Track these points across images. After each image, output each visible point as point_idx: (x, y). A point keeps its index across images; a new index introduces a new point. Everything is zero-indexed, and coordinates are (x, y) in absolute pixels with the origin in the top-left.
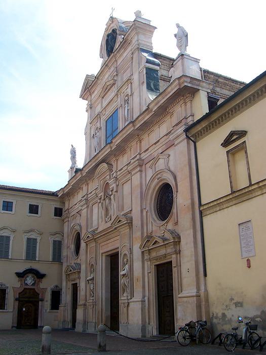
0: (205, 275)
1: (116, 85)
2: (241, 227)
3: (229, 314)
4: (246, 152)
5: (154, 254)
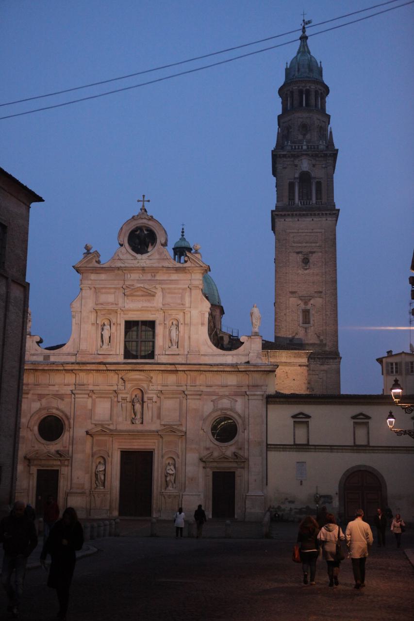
0: (267, 485)
3: (283, 507)
4: (308, 427)
5: (215, 464)
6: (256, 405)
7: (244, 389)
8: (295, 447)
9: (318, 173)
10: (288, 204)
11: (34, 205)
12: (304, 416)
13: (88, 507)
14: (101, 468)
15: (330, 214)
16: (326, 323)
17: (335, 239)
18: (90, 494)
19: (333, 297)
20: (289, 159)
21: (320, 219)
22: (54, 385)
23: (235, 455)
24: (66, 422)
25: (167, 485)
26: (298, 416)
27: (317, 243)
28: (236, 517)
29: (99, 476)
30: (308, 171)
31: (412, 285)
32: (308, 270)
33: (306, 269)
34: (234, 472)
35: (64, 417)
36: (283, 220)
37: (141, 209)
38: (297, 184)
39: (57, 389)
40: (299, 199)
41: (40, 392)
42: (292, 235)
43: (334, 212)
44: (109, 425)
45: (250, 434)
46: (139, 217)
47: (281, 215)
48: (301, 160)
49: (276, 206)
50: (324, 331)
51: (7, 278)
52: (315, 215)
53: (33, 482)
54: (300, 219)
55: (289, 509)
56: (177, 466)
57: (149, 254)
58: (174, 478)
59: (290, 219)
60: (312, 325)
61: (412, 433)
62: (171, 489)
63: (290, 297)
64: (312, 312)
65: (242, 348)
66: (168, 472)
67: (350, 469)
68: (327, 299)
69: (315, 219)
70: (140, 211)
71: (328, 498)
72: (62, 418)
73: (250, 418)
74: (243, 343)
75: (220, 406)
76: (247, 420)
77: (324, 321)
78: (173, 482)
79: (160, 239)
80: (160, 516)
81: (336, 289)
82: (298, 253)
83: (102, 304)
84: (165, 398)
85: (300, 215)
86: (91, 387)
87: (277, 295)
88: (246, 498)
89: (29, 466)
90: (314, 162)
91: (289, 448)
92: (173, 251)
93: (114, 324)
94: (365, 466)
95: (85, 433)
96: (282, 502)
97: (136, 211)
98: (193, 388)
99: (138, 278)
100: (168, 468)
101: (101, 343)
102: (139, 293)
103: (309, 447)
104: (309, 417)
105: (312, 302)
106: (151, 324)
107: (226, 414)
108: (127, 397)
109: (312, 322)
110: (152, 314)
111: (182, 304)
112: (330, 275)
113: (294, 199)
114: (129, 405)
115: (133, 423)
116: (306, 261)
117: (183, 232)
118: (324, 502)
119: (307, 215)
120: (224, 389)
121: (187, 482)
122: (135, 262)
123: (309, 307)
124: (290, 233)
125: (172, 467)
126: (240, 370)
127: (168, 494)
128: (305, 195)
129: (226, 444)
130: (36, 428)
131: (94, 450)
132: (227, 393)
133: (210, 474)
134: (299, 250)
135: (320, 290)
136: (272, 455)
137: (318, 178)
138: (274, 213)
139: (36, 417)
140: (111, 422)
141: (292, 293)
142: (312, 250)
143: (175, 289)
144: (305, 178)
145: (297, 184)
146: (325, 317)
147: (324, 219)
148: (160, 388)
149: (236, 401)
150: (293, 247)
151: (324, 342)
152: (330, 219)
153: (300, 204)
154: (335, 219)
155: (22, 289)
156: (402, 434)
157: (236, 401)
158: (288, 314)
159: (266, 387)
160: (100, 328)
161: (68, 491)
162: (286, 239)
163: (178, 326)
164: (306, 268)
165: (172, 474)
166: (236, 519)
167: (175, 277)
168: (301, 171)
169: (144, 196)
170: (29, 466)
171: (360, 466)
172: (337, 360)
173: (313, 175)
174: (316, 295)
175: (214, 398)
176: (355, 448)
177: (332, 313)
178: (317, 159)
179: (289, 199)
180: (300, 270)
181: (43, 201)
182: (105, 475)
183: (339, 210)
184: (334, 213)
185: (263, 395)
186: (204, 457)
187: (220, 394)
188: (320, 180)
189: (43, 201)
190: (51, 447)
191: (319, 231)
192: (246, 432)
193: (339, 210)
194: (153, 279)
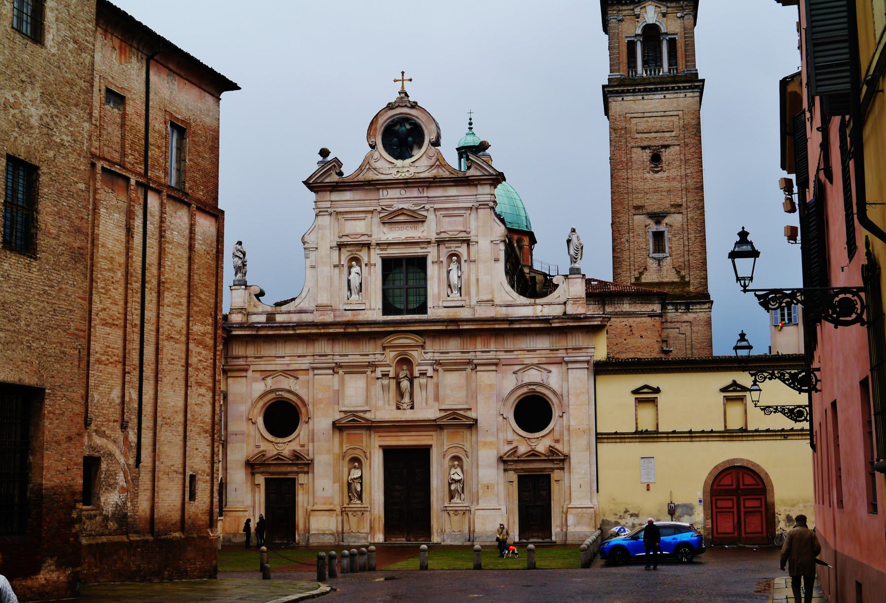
0: (598, 492)
1: (426, 224)
2: (643, 460)
6: (580, 377)
7: (562, 353)
8: (637, 436)
9: (670, 26)
10: (626, 75)
11: (225, 96)
12: (650, 391)
13: (340, 529)
14: (356, 473)
15: (690, 87)
16: (689, 251)
17: (699, 124)
18: (342, 512)
19: (698, 212)
20: (624, 8)
21: (675, 95)
22: (283, 357)
23: (552, 451)
24: (303, 410)
25: (452, 497)
26: (641, 391)
27: (673, 131)
28: (554, 538)
29: (353, 486)
30: (655, 24)
31: (785, 191)
32: (660, 173)
33: (657, 172)
34: (550, 475)
35: (299, 403)
36: (620, 99)
37: (400, 93)
38: (639, 44)
39: (289, 362)
40: (643, 66)
41: (263, 368)
42: (634, 121)
43: (696, 84)
44: (365, 412)
45: (571, 420)
46: (397, 104)
47: (617, 91)
48: (645, 7)
49: (609, 79)
50: (686, 263)
51: (189, 205)
52: (667, 89)
53: (261, 496)
54: (645, 97)
55: (631, 525)
56: (465, 468)
57: (413, 159)
58: (461, 486)
59: (631, 98)
60: (668, 255)
61: (787, 411)
62: (459, 501)
63: (634, 215)
64: (667, 235)
65: (556, 294)
66: (453, 476)
67: (720, 464)
68: (689, 215)
69: (668, 96)
70: (399, 96)
71: (689, 509)
72: (296, 404)
73: (570, 396)
74: (557, 286)
75: (526, 380)
76: (565, 398)
77: (686, 249)
78: (460, 492)
79: (429, 136)
80: (444, 541)
81: (702, 200)
82: (644, 148)
83: (347, 236)
84: (445, 370)
85: (645, 90)
86: (338, 359)
87: (615, 213)
88: (567, 512)
89: (253, 474)
90: (664, 9)
91: (629, 438)
92: (456, 152)
93: (366, 265)
94: (742, 460)
96: (620, 516)
97: (393, 97)
98: (485, 355)
99: (398, 196)
100: (453, 471)
101: (349, 293)
102: (402, 218)
103: (659, 435)
104: (657, 391)
105: (666, 220)
106: (420, 263)
107: (534, 391)
108: (389, 371)
109: (667, 250)
110: (422, 248)
111: (465, 231)
112: (694, 178)
113: (635, 67)
114: (393, 383)
115: (398, 408)
116: (656, 159)
117: (470, 124)
119: (656, 90)
120: (531, 355)
121: (480, 491)
122: (394, 171)
123: (662, 228)
124: (631, 118)
125: (459, 470)
126: (553, 325)
127: (455, 509)
128: (652, 60)
129: (537, 435)
130: (260, 421)
131: (345, 449)
132: (536, 361)
133: (514, 477)
134: (645, 144)
135: (679, 201)
136: (603, 447)
137: (671, 34)
138: (606, 90)
139: (261, 403)
141: (637, 208)
142: (666, 143)
143: (454, 209)
144: (651, 33)
145: (639, 44)
146: (686, 243)
147: (682, 95)
148: (437, 356)
149: (550, 372)
150: (636, 138)
151: (687, 279)
152: (691, 94)
153: (645, 75)
154: (698, 94)
155: (213, 220)
156: (771, 412)
157: (550, 372)
158: (632, 240)
159: (592, 350)
160: (346, 269)
161: (310, 508)
162: (626, 128)
163: (459, 261)
164: (656, 169)
165: (459, 481)
166: (555, 542)
167: (453, 191)
168: (645, 24)
169: (403, 73)
170: (253, 474)
171: (733, 460)
172: (707, 306)
173: (663, 30)
174: (673, 210)
175: (517, 368)
176: (726, 434)
177: (697, 235)
178: (669, 5)
179: (629, 67)
180: (649, 172)
181: (239, 88)
182: (361, 484)
183: (703, 81)
184: (696, 85)
185: (588, 362)
186: (505, 454)
187: (527, 361)
188: (675, 36)
189: (239, 88)
190: (282, 446)
191: (675, 113)
192: (564, 415)
193: (703, 81)
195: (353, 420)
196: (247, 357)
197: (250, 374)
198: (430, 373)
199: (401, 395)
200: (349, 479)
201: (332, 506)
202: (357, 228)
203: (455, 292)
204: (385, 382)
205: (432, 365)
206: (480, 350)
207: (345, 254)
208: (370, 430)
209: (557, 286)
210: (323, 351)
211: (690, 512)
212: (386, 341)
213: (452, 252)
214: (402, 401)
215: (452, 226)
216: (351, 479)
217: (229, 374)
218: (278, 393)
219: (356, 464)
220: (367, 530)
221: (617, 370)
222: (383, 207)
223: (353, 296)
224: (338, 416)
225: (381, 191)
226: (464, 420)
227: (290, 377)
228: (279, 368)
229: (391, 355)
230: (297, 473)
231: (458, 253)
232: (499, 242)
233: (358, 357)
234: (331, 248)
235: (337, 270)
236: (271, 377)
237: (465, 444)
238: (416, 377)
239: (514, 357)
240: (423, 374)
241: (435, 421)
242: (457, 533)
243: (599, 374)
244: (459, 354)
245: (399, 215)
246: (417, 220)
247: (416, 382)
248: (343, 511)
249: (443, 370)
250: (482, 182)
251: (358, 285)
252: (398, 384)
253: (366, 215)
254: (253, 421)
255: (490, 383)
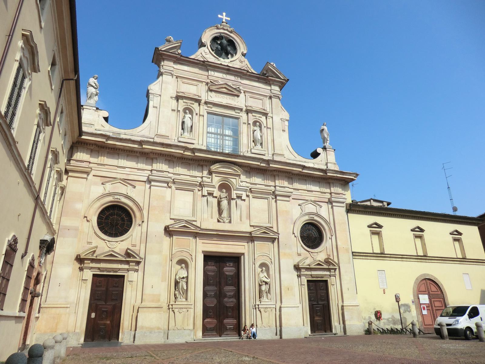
2: (379, 272)
24: (138, 214)
62: (267, 300)
74: (319, 154)
75: (307, 211)
93: (197, 114)
95: (163, 231)
114: (215, 201)
115: (219, 221)
118: (405, 312)
126: (328, 174)
127: (265, 306)
132: (313, 199)
139: (98, 204)
140: (194, 219)
149: (321, 207)
163: (260, 127)
170: (81, 269)
182: (187, 283)
194: (235, 80)
195: (185, 226)
196: (90, 163)
197: (90, 176)
198: (244, 197)
199: (220, 212)
200: (177, 277)
201: (160, 304)
202: (191, 90)
203: (259, 146)
204: (210, 198)
205: (246, 191)
206: (282, 185)
207: (182, 104)
208: (196, 237)
209: (319, 154)
210: (161, 168)
211: (409, 310)
212: (214, 167)
213: (256, 120)
214: (223, 216)
215: (256, 104)
216: (180, 278)
217: (70, 174)
218: (116, 197)
219: (183, 265)
220: (191, 327)
221: (360, 211)
222: (212, 81)
223: (186, 134)
224: (169, 222)
225: (210, 72)
226: (272, 234)
227: (128, 185)
228: (118, 176)
229: (216, 180)
230: (128, 270)
231: (262, 123)
232: (285, 120)
233: (188, 177)
234: (171, 98)
235: (175, 113)
236: (110, 183)
237: (270, 254)
238: (233, 199)
239: (299, 194)
240: (239, 197)
241: (250, 233)
242: (267, 328)
243: (349, 213)
244: (264, 187)
245: (222, 88)
246: (234, 93)
247: (233, 203)
248: (170, 308)
249: (252, 197)
250: (275, 83)
251: (190, 126)
252: (219, 203)
253: (199, 84)
254: (88, 219)
255: (286, 210)
